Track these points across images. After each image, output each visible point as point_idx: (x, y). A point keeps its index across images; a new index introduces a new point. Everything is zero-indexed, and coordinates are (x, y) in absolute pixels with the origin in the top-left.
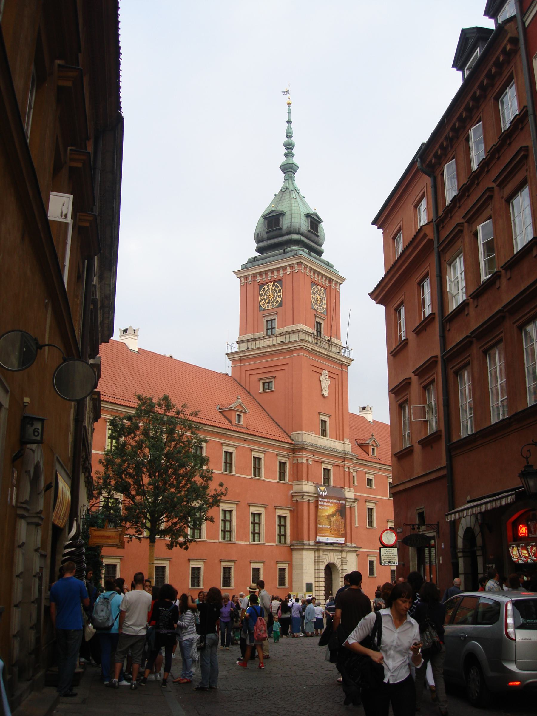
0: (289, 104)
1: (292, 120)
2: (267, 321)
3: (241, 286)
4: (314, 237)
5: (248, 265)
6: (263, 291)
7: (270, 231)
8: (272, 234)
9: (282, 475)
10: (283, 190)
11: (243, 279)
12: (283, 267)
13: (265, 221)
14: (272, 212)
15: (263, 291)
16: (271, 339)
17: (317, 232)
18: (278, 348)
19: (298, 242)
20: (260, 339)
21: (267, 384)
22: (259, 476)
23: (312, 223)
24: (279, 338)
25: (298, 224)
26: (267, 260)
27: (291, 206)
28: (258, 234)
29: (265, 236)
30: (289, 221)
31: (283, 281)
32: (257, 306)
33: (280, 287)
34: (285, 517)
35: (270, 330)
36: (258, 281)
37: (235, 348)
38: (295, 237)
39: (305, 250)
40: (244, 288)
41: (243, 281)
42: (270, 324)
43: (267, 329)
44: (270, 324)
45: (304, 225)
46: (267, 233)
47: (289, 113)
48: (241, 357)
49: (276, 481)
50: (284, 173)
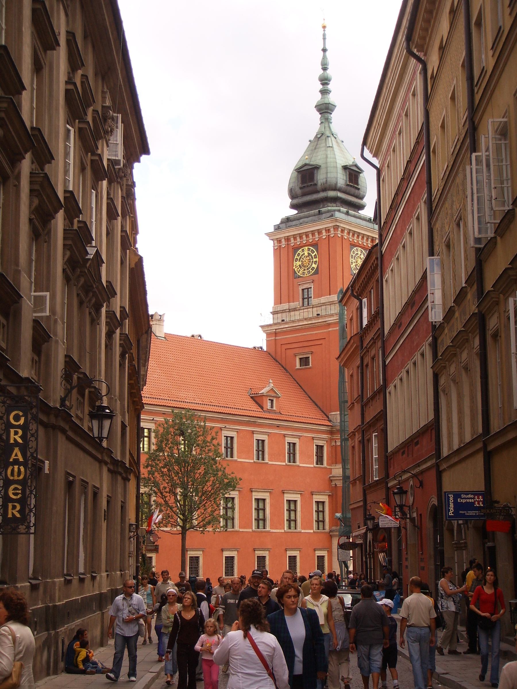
0: (324, 27)
1: (327, 47)
3: (274, 249)
4: (353, 190)
5: (281, 226)
6: (298, 256)
7: (304, 186)
8: (307, 190)
9: (320, 460)
10: (319, 136)
11: (276, 242)
12: (318, 230)
13: (298, 175)
14: (306, 165)
17: (357, 183)
18: (314, 322)
19: (335, 200)
20: (295, 310)
21: (305, 361)
22: (294, 462)
23: (350, 175)
24: (315, 309)
25: (334, 179)
26: (301, 221)
27: (327, 157)
29: (299, 191)
30: (325, 176)
33: (316, 252)
34: (323, 503)
35: (307, 300)
36: (292, 245)
37: (269, 320)
38: (332, 194)
39: (342, 209)
40: (278, 251)
41: (276, 244)
42: (307, 293)
43: (303, 299)
44: (306, 294)
45: (341, 179)
46: (301, 188)
47: (324, 39)
48: (276, 329)
49: (312, 466)
50: (320, 114)
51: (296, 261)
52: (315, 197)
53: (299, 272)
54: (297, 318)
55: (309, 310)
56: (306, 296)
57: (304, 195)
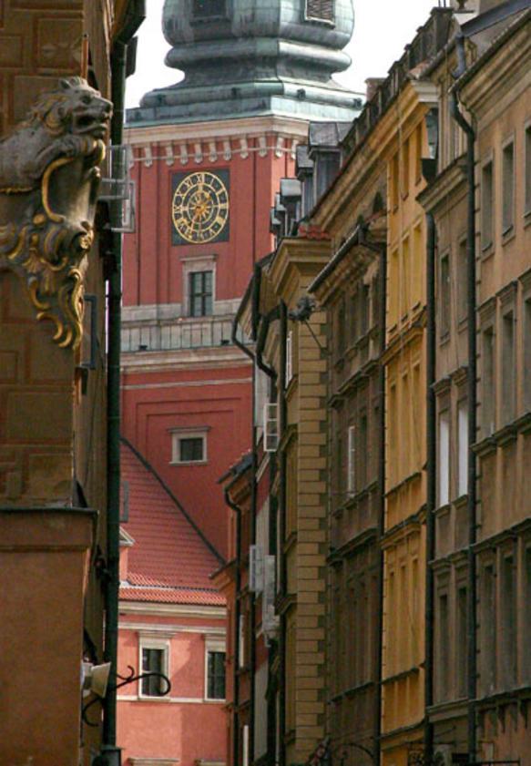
2: (192, 275)
5: (143, 113)
7: (201, 22)
15: (183, 191)
16: (197, 326)
26: (192, 108)
28: (171, 39)
29: (189, 32)
31: (232, 171)
32: (165, 229)
33: (224, 189)
36: (169, 163)
43: (193, 296)
44: (198, 284)
46: (192, 24)
49: (199, 701)
51: (178, 204)
52: (223, 49)
53: (183, 232)
54: (176, 343)
55: (204, 326)
56: (198, 291)
57: (200, 40)
